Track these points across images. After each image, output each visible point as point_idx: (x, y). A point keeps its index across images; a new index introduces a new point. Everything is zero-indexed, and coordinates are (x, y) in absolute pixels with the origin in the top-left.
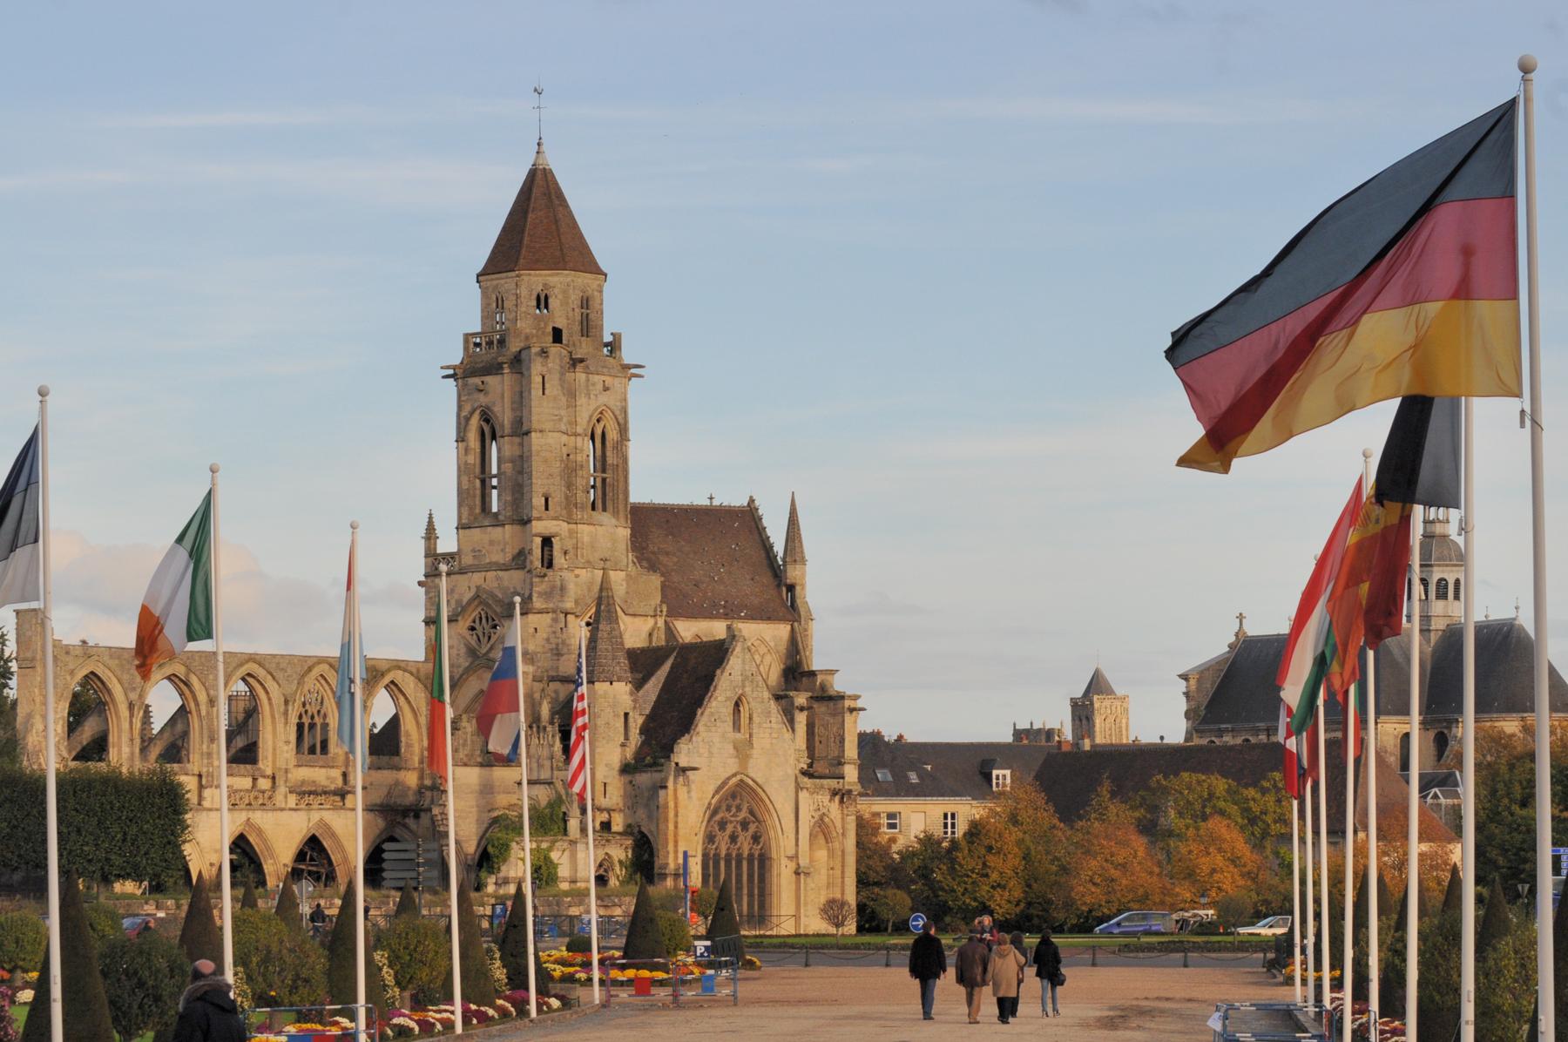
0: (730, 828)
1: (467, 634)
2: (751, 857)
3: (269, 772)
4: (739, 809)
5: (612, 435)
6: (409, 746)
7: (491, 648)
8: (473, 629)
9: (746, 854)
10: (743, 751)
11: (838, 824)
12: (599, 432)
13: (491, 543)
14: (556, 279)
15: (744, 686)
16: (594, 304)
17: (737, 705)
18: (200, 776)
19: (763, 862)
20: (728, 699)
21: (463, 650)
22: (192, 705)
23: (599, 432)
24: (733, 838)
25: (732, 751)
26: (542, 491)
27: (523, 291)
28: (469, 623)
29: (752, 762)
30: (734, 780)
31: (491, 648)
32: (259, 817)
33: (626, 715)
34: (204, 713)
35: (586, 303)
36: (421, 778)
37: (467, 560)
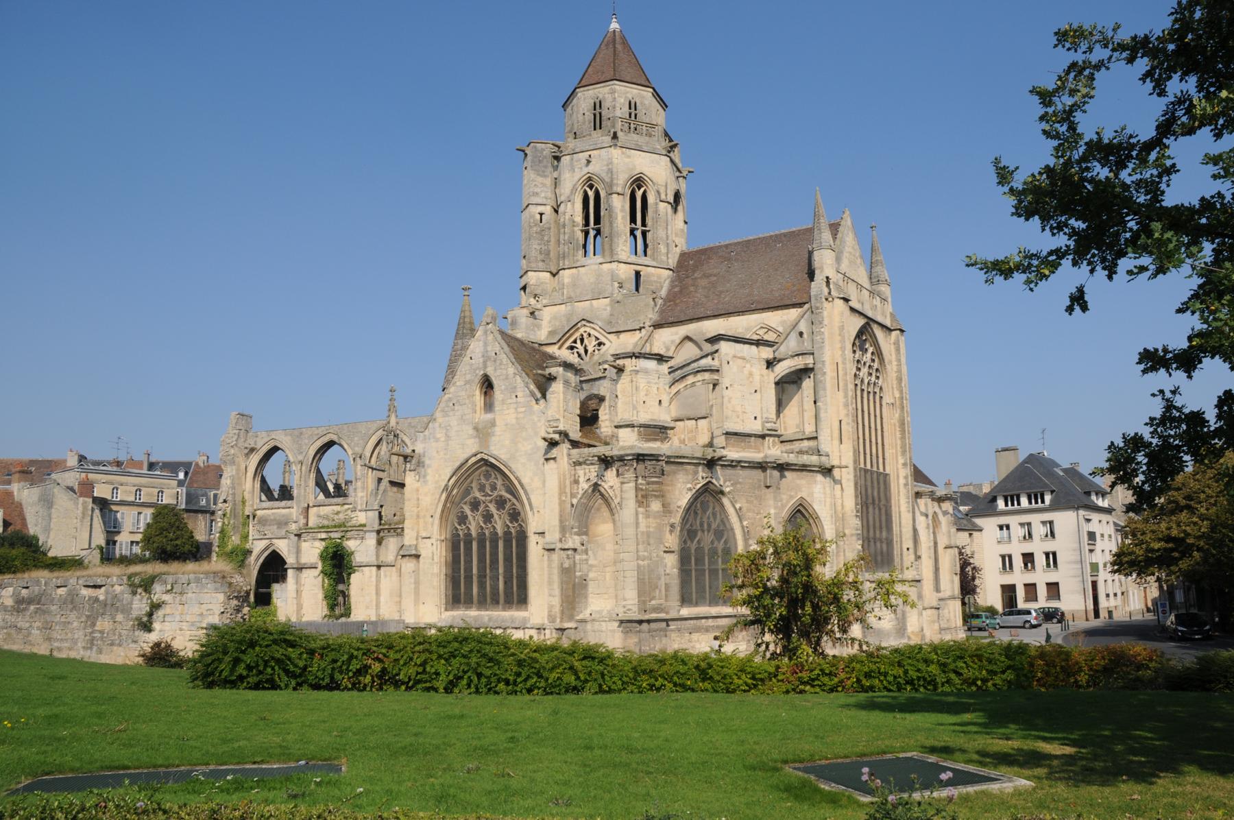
0: (481, 508)
2: (507, 534)
4: (494, 488)
5: (603, 194)
9: (500, 531)
10: (483, 433)
11: (618, 492)
12: (591, 194)
15: (485, 367)
16: (605, 105)
17: (487, 385)
19: (522, 538)
20: (467, 382)
23: (591, 194)
24: (488, 517)
25: (471, 432)
29: (494, 439)
30: (474, 459)
35: (598, 105)
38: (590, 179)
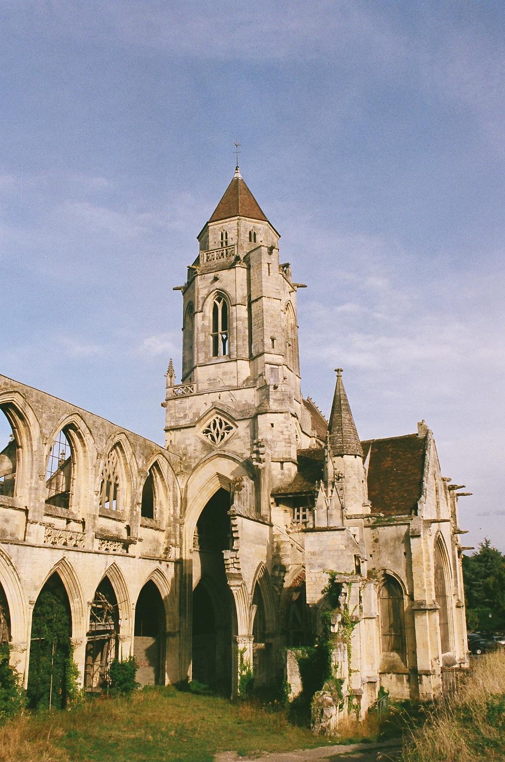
1: (203, 436)
3: (80, 518)
6: (161, 512)
7: (226, 443)
8: (207, 432)
13: (225, 373)
14: (259, 226)
18: (26, 511)
21: (199, 446)
22: (25, 440)
26: (270, 335)
27: (242, 229)
28: (204, 427)
31: (226, 443)
32: (71, 557)
33: (363, 481)
34: (35, 448)
36: (168, 537)
37: (203, 386)
38: (287, 306)
